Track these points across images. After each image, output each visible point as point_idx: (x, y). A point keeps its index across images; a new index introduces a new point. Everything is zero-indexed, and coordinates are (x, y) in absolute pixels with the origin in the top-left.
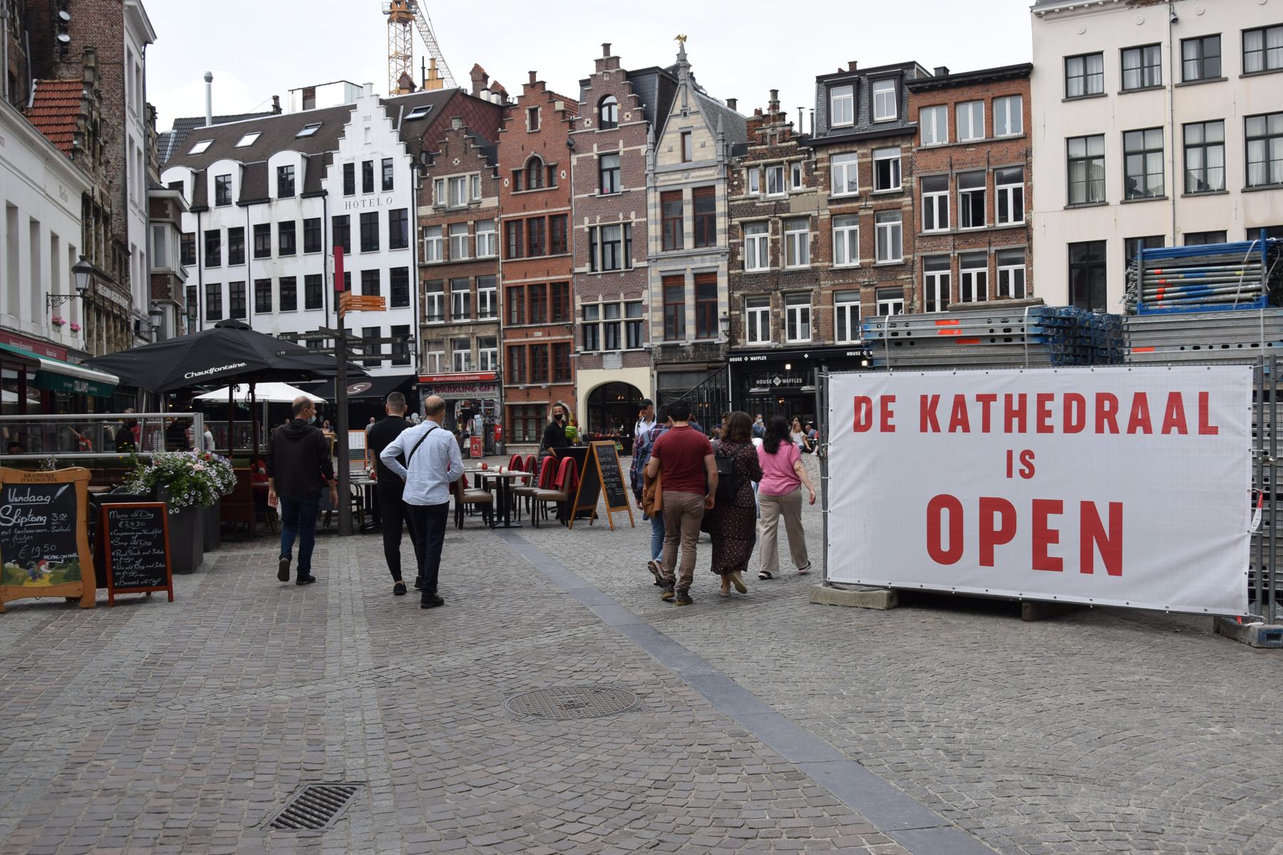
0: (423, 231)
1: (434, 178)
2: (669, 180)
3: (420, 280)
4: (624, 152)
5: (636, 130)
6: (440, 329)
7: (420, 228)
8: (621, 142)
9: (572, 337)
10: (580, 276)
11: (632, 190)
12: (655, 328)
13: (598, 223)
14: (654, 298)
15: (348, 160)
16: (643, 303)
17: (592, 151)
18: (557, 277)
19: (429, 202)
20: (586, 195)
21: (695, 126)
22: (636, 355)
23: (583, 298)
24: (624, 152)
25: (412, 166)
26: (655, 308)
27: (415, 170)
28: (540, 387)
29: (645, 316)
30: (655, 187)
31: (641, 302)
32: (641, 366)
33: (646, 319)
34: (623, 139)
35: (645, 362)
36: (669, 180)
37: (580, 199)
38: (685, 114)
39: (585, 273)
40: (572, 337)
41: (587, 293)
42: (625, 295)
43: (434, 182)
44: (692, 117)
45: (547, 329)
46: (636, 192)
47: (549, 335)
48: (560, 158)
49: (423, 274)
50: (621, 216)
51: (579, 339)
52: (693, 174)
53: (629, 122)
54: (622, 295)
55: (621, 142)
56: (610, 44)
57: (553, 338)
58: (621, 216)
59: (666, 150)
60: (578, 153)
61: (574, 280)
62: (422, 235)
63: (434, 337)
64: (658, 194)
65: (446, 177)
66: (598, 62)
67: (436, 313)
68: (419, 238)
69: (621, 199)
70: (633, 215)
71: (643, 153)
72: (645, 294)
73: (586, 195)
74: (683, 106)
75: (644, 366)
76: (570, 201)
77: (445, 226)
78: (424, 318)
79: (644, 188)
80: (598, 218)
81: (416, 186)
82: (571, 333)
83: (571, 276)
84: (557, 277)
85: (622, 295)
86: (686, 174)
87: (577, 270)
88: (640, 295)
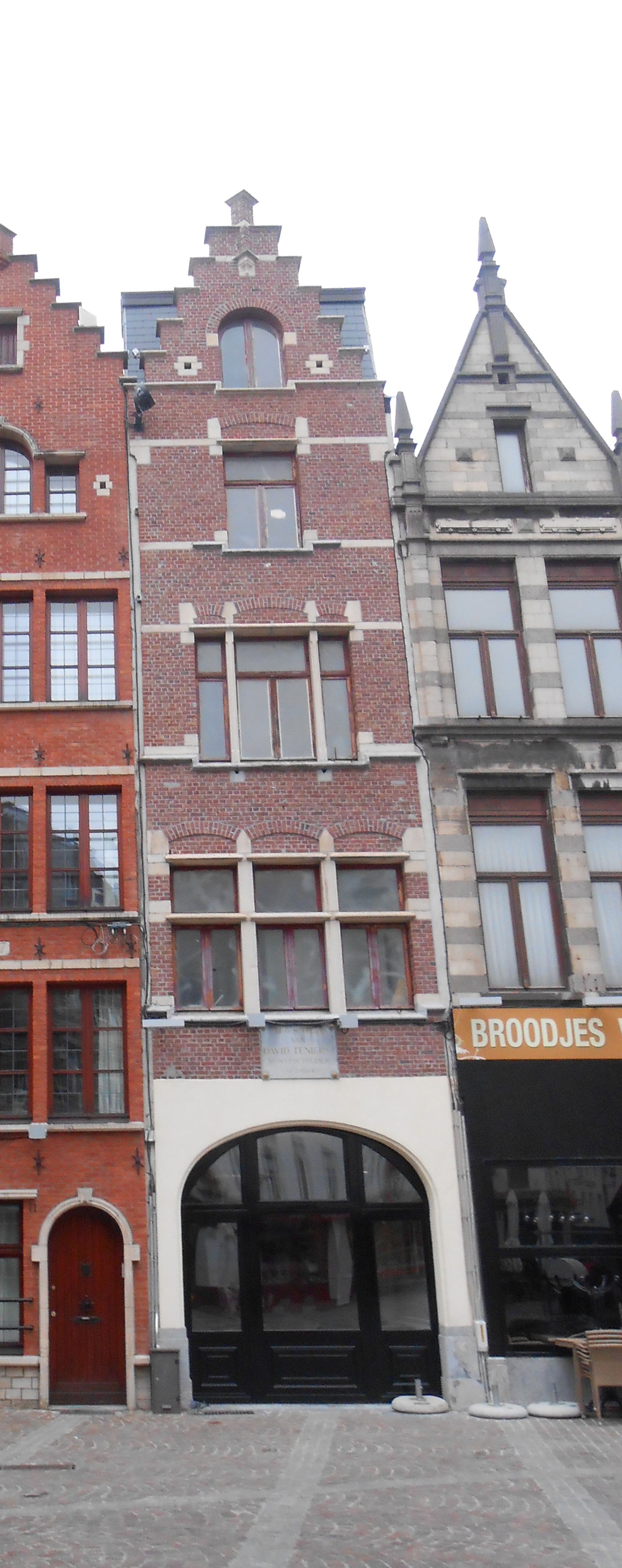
2: (469, 530)
4: (313, 447)
5: (351, 399)
8: (302, 426)
9: (134, 963)
10: (158, 772)
11: (346, 544)
12: (456, 949)
13: (230, 623)
14: (447, 856)
16: (408, 868)
17: (204, 434)
18: (77, 771)
20: (187, 545)
21: (535, 407)
22: (391, 1034)
23: (174, 841)
24: (313, 447)
26: (451, 883)
28: (24, 1135)
29: (416, 909)
30: (428, 542)
31: (398, 866)
32: (414, 1073)
33: (420, 916)
34: (310, 417)
35: (426, 1061)
36: (469, 530)
37: (161, 554)
38: (503, 379)
39: (189, 762)
40: (134, 963)
41: (190, 824)
42: (339, 840)
44: (523, 387)
45: (31, 932)
46: (360, 551)
47: (40, 954)
48: (89, 443)
50: (311, 610)
51: (160, 973)
52: (546, 523)
53: (324, 376)
54: (326, 838)
55: (302, 426)
56: (257, 202)
57: (57, 964)
58: (311, 610)
59: (452, 454)
60: (156, 436)
61: (140, 783)
64: (436, 564)
66: (212, 234)
69: (309, 562)
70: (353, 612)
71: (376, 455)
72: (410, 836)
73: (187, 545)
74: (498, 358)
75: (427, 1071)
76: (124, 557)
79: (388, 543)
80: (230, 610)
82: (131, 950)
83: (131, 769)
84: (77, 771)
85: (326, 838)
86: (524, 522)
87: (152, 753)
88: (398, 840)
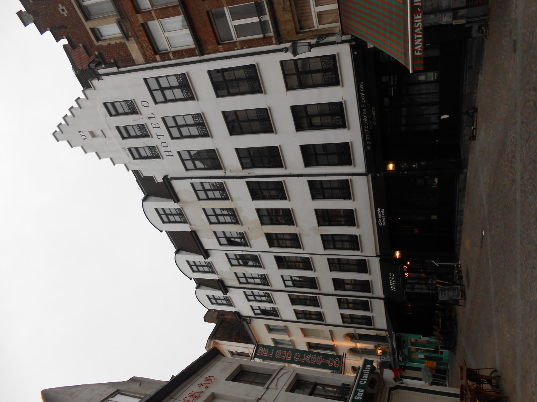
0: (160, 54)
1: (96, 44)
3: (218, 51)
6: (276, 6)
7: (158, 57)
15: (128, 155)
19: (123, 46)
25: (99, 77)
27: (101, 71)
43: (100, 43)
49: (210, 47)
62: (165, 56)
63: (289, 16)
65: (88, 25)
67: (256, 19)
68: (169, 59)
77: (140, 19)
78: (266, 41)
81: (114, 69)
